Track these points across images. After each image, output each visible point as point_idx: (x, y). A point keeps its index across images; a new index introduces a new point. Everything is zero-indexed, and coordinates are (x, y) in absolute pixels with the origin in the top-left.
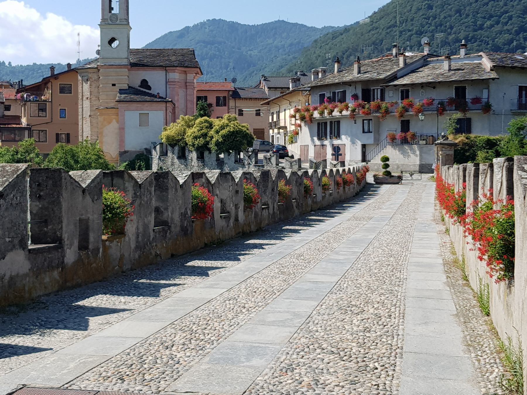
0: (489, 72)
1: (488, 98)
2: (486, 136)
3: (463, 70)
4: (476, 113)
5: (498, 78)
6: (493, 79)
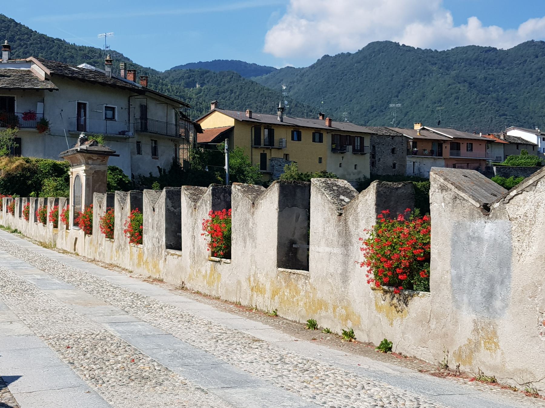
0: (43, 82)
1: (43, 114)
2: (50, 161)
3: (9, 76)
4: (29, 132)
5: (57, 90)
6: (51, 90)
